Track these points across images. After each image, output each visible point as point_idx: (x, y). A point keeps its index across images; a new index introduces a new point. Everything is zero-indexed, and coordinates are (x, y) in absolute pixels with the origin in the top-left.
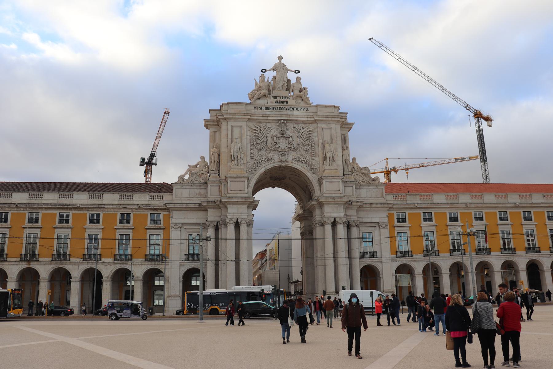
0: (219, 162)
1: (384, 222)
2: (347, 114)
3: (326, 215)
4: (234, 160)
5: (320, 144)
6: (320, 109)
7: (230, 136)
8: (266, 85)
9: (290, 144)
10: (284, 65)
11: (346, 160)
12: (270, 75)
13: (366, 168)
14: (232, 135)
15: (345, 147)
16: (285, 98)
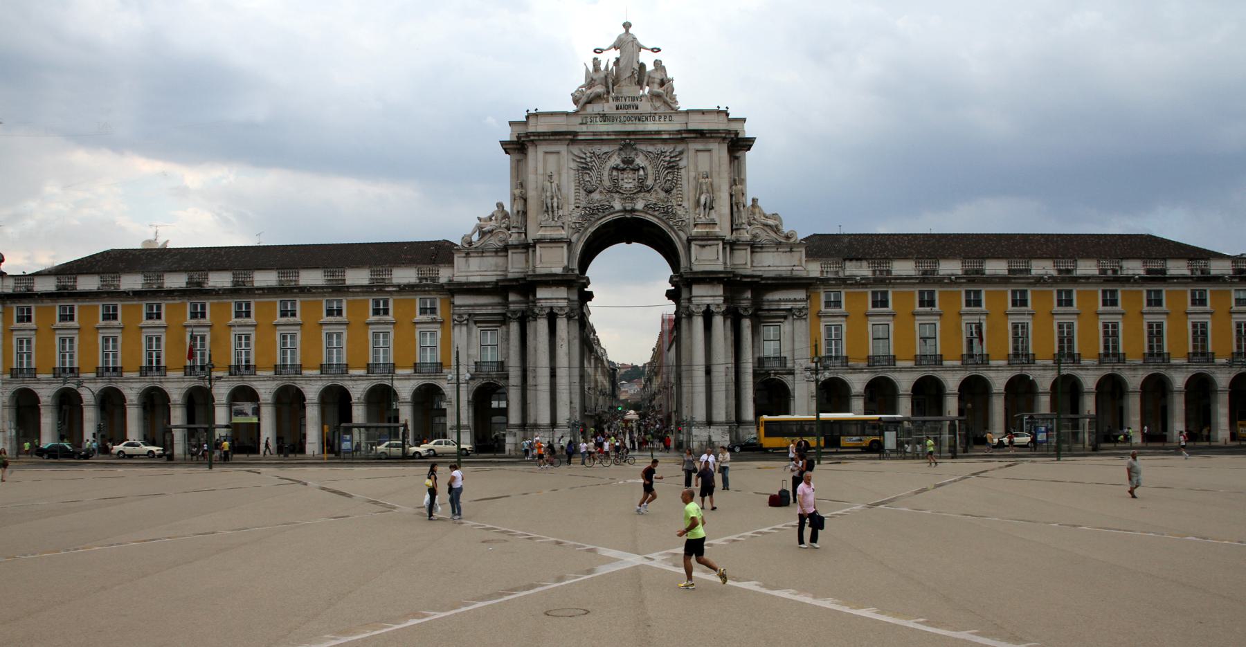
0: (525, 213)
1: (800, 310)
2: (744, 120)
3: (695, 301)
4: (547, 211)
5: (691, 179)
6: (691, 116)
7: (540, 171)
8: (602, 75)
9: (642, 181)
10: (635, 39)
11: (737, 204)
12: (609, 58)
13: (775, 216)
14: (545, 169)
15: (737, 179)
16: (633, 99)
